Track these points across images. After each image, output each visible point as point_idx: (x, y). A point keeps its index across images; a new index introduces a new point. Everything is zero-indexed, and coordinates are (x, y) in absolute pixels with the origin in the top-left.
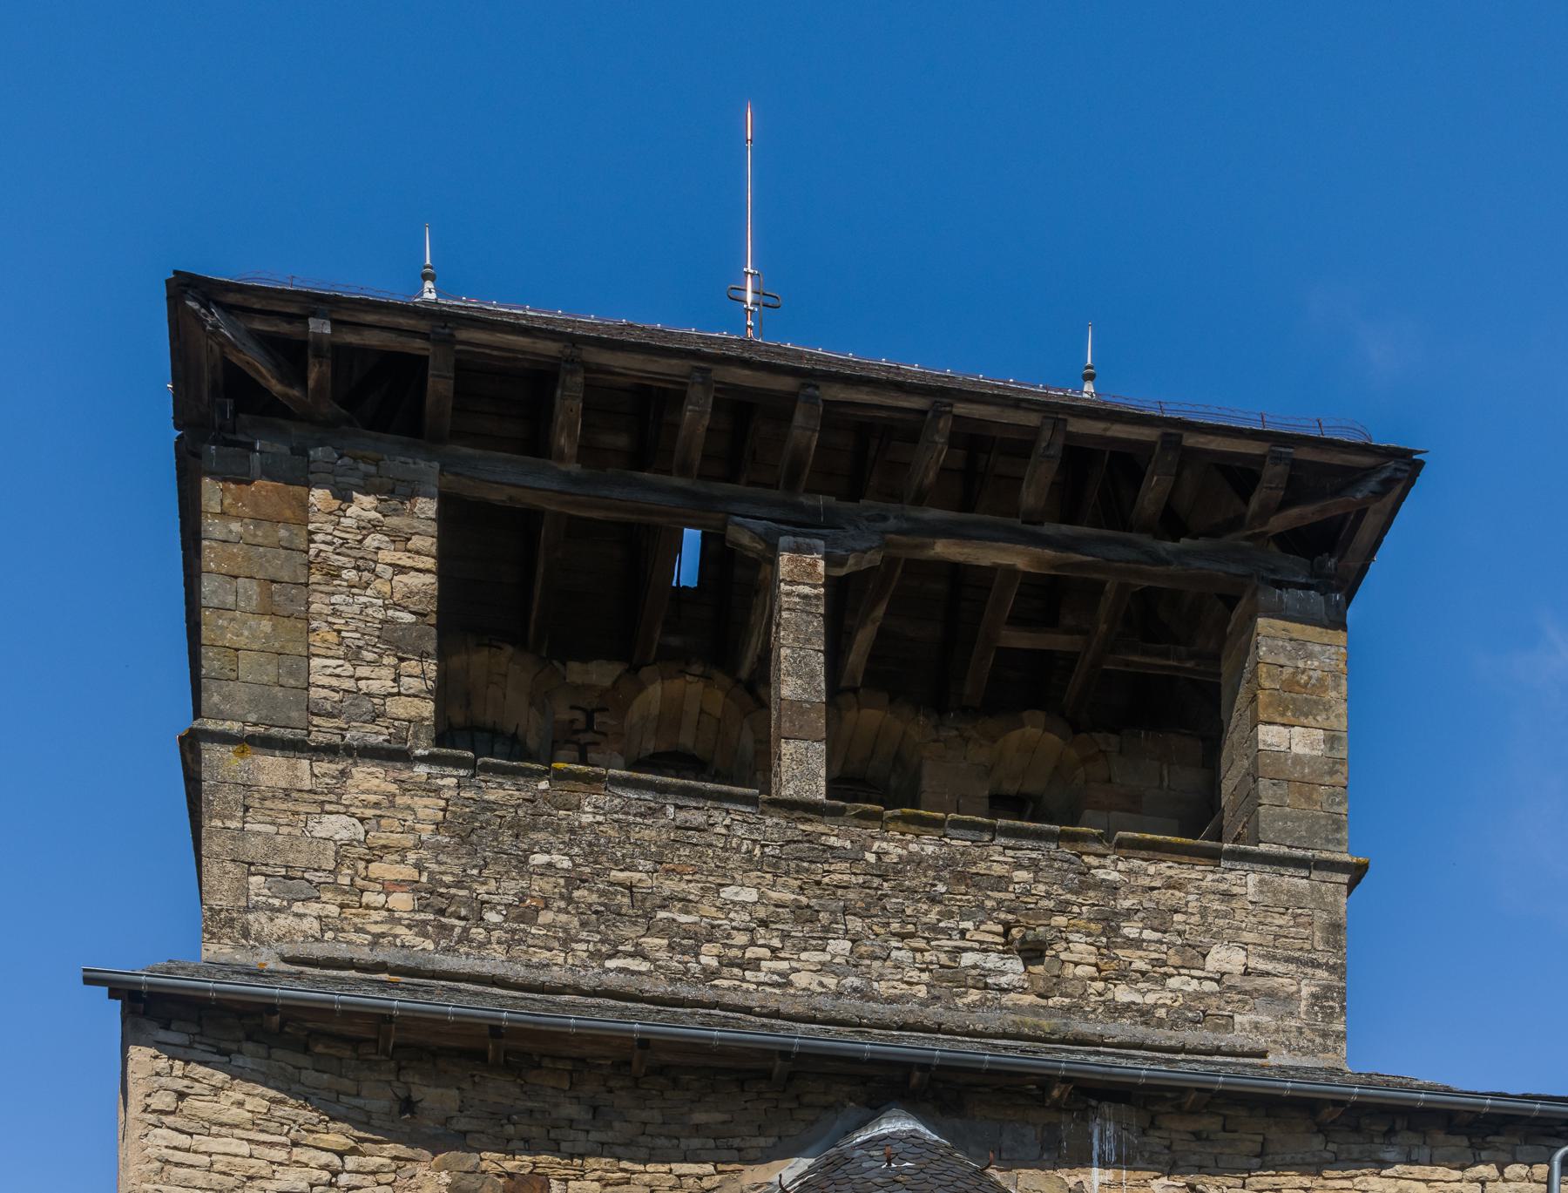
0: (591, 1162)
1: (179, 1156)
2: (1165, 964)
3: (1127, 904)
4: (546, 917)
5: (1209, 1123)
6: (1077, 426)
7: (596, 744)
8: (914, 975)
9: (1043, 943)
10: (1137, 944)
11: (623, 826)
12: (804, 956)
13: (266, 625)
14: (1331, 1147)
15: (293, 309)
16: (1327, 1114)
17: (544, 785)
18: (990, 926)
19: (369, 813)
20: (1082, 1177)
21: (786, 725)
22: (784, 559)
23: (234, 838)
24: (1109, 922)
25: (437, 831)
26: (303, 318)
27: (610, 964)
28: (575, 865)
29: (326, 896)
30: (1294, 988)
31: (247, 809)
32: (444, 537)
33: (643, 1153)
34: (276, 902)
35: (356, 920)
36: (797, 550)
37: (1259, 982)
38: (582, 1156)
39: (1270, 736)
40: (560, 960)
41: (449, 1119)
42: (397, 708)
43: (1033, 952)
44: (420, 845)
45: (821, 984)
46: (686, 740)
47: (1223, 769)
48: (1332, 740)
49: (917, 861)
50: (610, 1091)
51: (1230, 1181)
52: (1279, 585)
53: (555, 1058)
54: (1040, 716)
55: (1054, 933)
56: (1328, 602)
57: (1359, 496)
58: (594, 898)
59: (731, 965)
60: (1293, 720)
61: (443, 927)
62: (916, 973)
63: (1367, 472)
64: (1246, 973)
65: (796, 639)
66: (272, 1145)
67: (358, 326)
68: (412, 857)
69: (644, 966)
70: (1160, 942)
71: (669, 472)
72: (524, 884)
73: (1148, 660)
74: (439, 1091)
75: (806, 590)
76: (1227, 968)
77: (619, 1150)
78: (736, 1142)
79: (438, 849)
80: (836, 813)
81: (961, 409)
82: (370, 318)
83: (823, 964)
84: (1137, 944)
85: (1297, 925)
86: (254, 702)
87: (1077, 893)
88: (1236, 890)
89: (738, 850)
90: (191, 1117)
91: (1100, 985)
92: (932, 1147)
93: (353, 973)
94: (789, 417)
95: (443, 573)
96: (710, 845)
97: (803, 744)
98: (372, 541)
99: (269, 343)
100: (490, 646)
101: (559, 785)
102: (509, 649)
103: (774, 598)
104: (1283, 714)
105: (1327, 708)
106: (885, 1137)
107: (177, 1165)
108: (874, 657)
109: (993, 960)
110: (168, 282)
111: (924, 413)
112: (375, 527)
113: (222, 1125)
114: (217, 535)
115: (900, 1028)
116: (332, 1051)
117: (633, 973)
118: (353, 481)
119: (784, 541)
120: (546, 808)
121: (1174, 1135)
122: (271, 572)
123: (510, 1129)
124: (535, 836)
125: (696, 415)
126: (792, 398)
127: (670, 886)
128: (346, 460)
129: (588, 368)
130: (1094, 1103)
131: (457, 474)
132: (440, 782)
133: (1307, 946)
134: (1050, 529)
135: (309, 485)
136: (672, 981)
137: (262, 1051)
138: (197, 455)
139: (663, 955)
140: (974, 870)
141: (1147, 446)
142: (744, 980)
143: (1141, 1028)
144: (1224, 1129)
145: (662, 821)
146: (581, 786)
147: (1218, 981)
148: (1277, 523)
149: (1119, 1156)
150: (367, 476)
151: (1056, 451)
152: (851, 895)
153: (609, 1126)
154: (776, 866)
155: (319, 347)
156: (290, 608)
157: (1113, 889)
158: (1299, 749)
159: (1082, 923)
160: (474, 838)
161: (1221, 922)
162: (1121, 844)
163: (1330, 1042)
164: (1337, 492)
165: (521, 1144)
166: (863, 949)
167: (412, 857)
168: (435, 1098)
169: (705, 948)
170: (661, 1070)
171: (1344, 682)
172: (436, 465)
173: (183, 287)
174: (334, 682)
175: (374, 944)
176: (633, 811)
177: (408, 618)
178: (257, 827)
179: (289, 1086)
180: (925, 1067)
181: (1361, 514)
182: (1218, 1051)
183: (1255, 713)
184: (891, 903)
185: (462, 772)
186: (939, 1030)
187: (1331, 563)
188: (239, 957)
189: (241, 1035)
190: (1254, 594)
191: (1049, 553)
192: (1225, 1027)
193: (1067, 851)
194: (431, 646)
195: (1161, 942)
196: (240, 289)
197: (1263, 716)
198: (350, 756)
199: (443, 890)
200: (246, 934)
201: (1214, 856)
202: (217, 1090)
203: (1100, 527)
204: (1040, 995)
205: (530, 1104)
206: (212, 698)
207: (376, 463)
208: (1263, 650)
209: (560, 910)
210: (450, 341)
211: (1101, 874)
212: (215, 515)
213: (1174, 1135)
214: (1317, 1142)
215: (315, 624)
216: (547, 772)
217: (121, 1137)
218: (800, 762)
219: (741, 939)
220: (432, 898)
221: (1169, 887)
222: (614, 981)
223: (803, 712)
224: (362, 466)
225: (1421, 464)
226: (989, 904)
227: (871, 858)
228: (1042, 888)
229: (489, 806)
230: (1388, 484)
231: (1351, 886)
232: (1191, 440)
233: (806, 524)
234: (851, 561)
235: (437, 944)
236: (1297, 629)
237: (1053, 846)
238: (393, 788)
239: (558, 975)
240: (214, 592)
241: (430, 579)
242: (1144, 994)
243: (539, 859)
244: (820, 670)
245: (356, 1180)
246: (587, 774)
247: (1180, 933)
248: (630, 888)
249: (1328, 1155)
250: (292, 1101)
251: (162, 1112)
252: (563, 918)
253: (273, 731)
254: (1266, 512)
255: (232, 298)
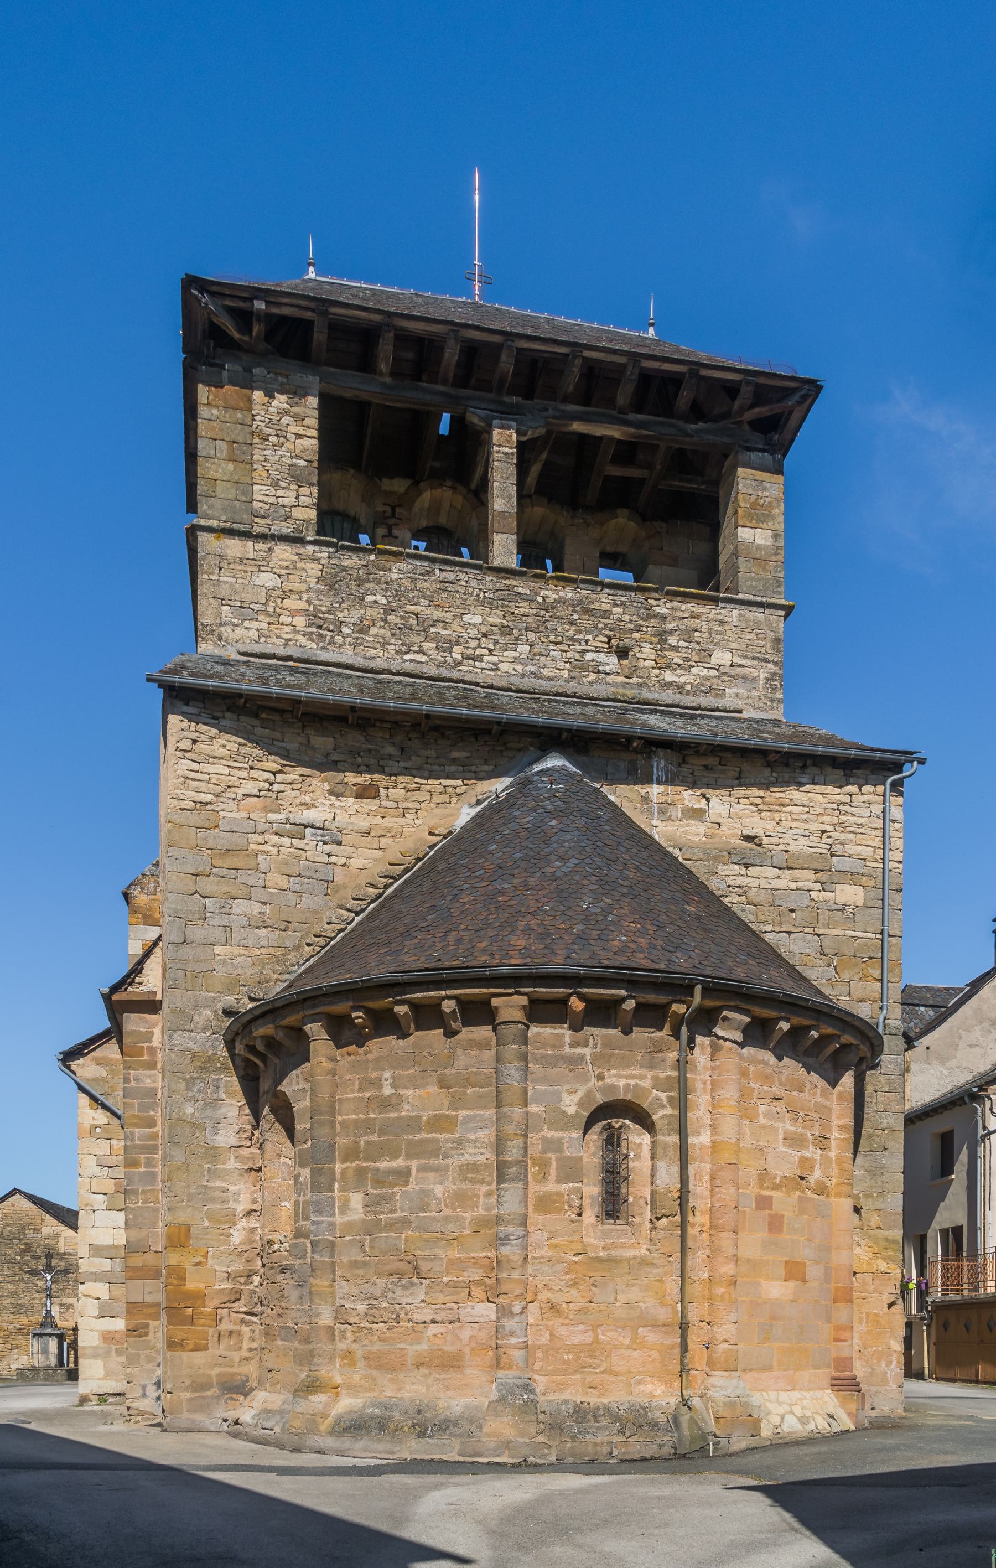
0: (400, 778)
1: (193, 775)
2: (690, 660)
3: (671, 626)
4: (373, 631)
5: (712, 761)
6: (646, 364)
7: (396, 525)
8: (562, 665)
9: (627, 648)
10: (676, 648)
11: (413, 581)
12: (505, 653)
13: (230, 466)
14: (775, 774)
15: (245, 295)
16: (772, 757)
17: (372, 557)
18: (601, 638)
19: (283, 572)
20: (648, 790)
21: (496, 525)
22: (496, 432)
23: (214, 585)
24: (662, 636)
25: (318, 583)
26: (251, 300)
27: (407, 657)
28: (389, 602)
29: (261, 618)
30: (756, 674)
31: (220, 569)
32: (322, 419)
33: (426, 774)
34: (236, 621)
35: (276, 631)
36: (502, 427)
37: (739, 670)
38: (396, 775)
39: (744, 534)
40: (381, 655)
41: (329, 754)
42: (297, 513)
43: (623, 653)
44: (309, 590)
45: (514, 669)
46: (443, 520)
47: (720, 549)
48: (776, 536)
49: (563, 601)
50: (410, 740)
51: (723, 793)
52: (749, 449)
53: (382, 721)
54: (626, 511)
55: (633, 642)
56: (774, 459)
57: (790, 403)
58: (398, 620)
59: (468, 658)
60: (756, 525)
61: (321, 636)
62: (563, 664)
63: (794, 391)
64: (732, 666)
65: (502, 477)
66: (240, 768)
67: (279, 305)
68: (305, 596)
69: (424, 659)
70: (688, 648)
71: (436, 383)
72: (362, 612)
73: (681, 484)
74: (324, 739)
75: (507, 450)
76: (722, 662)
77: (414, 772)
78: (473, 768)
79: (319, 592)
80: (522, 574)
81: (587, 354)
82: (285, 300)
83: (515, 658)
84: (676, 648)
85: (758, 639)
86: (224, 509)
87: (645, 620)
88: (726, 619)
89: (471, 595)
90: (200, 754)
91: (657, 671)
92: (571, 775)
93: (274, 662)
94: (499, 357)
95: (321, 439)
96: (457, 592)
97: (505, 536)
98: (285, 420)
99: (232, 311)
100: (342, 469)
101: (381, 557)
102: (352, 471)
103: (489, 453)
104: (751, 522)
105: (774, 518)
106: (549, 769)
107: (192, 779)
108: (542, 475)
109: (602, 657)
110: (182, 280)
111: (567, 355)
112: (286, 413)
113: (215, 758)
114: (206, 417)
115: (555, 695)
116: (270, 717)
117: (418, 662)
118: (275, 387)
119: (495, 422)
120: (374, 570)
121: (695, 768)
122: (233, 437)
123: (359, 760)
124: (368, 585)
125: (451, 354)
126: (499, 347)
127: (437, 614)
128: (272, 375)
129: (396, 328)
130: (654, 749)
131: (328, 383)
132: (320, 555)
133: (763, 651)
134: (632, 417)
135: (252, 389)
136: (438, 667)
137: (235, 717)
138: (195, 369)
139: (433, 652)
140: (592, 607)
141: (682, 374)
142: (474, 667)
143: (678, 696)
144: (720, 764)
145: (433, 578)
146: (392, 558)
147: (717, 670)
148: (750, 415)
149: (667, 778)
150: (282, 384)
151: (635, 377)
152: (530, 620)
153: (410, 759)
154: (491, 603)
155: (260, 316)
156: (243, 457)
157: (664, 618)
158: (758, 541)
159: (648, 637)
160: (337, 586)
161: (719, 637)
162: (668, 593)
163: (775, 704)
164: (779, 401)
165: (365, 768)
166: (535, 650)
167: (305, 596)
168: (322, 742)
169: (455, 648)
170: (436, 728)
171: (782, 504)
172: (318, 378)
173: (190, 282)
174: (266, 499)
175: (285, 645)
176: (418, 572)
177: (303, 463)
178: (226, 579)
179: (249, 736)
180: (569, 730)
181: (791, 412)
182: (717, 709)
183: (736, 521)
184: (550, 625)
185: (331, 550)
186: (574, 696)
187: (776, 437)
188: (217, 652)
189: (225, 708)
190: (736, 453)
191: (631, 430)
192: (721, 695)
193: (640, 597)
194: (315, 479)
195: (688, 648)
196: (219, 284)
197: (740, 523)
198: (274, 540)
199: (321, 615)
200: (220, 639)
201: (715, 600)
202: (212, 738)
203: (659, 416)
204: (626, 677)
205: (369, 746)
206: (203, 507)
207: (287, 377)
208: (740, 486)
209: (380, 627)
210: (326, 313)
211: (657, 610)
212: (204, 405)
213: (695, 768)
214: (767, 772)
215: (255, 466)
216: (374, 550)
217: (162, 760)
218: (504, 546)
219: (473, 644)
220: (317, 621)
221: (692, 617)
222: (409, 667)
223: (505, 518)
224: (280, 378)
225: (820, 388)
226: (600, 626)
227: (540, 599)
228: (627, 618)
229: (345, 569)
230: (804, 397)
231: (785, 617)
232: (704, 372)
233: (507, 413)
234: (530, 433)
235: (318, 645)
236: (759, 474)
237: (633, 594)
238: (296, 558)
239: (379, 664)
240: (204, 448)
241: (315, 442)
242: (679, 677)
243: (370, 598)
244: (514, 494)
245: (282, 787)
246: (395, 552)
247: (698, 643)
248: (417, 615)
249: (772, 779)
250: (250, 745)
251: (185, 751)
252: (382, 631)
253: (234, 526)
254: (742, 410)
255: (215, 288)
